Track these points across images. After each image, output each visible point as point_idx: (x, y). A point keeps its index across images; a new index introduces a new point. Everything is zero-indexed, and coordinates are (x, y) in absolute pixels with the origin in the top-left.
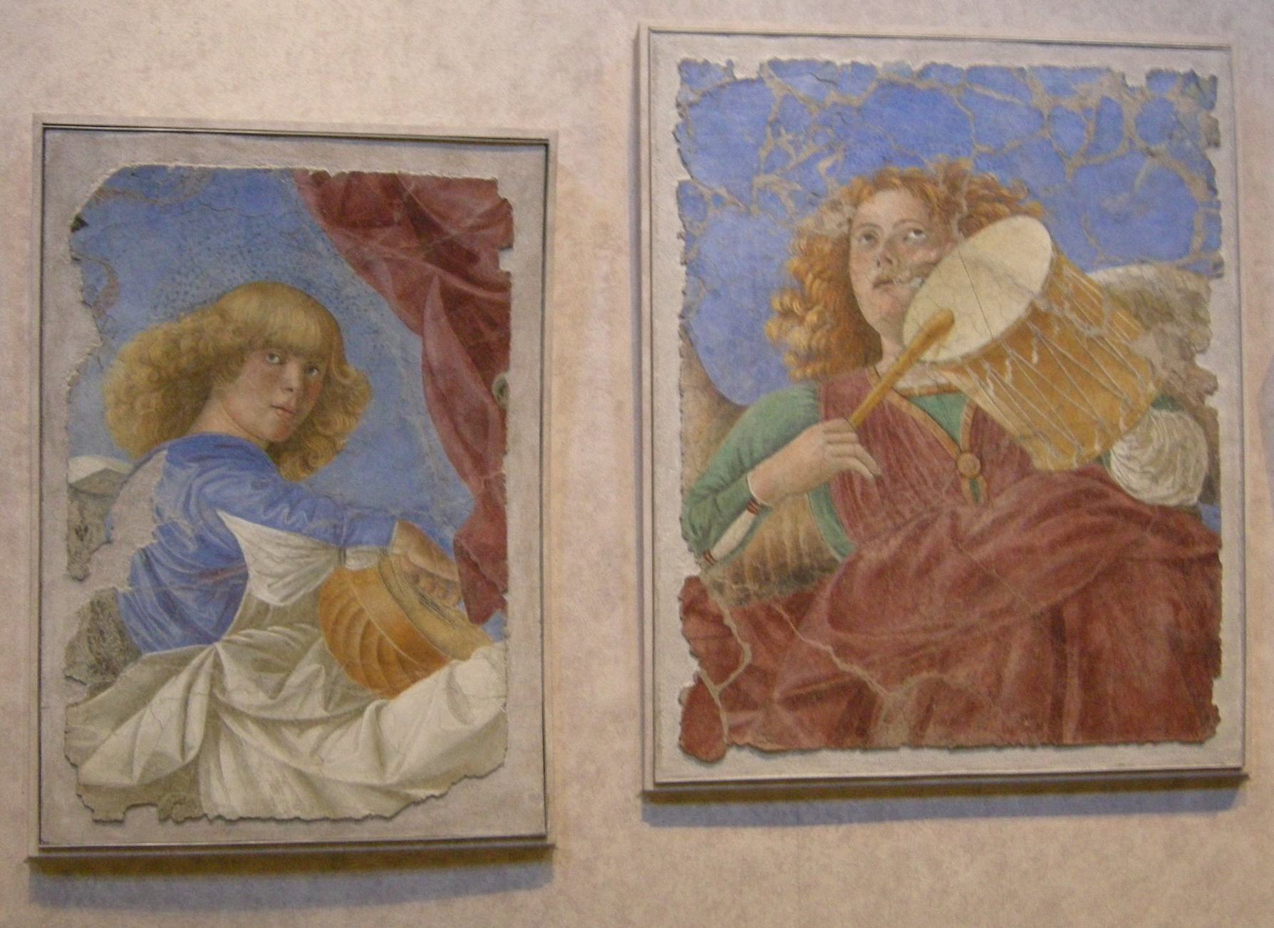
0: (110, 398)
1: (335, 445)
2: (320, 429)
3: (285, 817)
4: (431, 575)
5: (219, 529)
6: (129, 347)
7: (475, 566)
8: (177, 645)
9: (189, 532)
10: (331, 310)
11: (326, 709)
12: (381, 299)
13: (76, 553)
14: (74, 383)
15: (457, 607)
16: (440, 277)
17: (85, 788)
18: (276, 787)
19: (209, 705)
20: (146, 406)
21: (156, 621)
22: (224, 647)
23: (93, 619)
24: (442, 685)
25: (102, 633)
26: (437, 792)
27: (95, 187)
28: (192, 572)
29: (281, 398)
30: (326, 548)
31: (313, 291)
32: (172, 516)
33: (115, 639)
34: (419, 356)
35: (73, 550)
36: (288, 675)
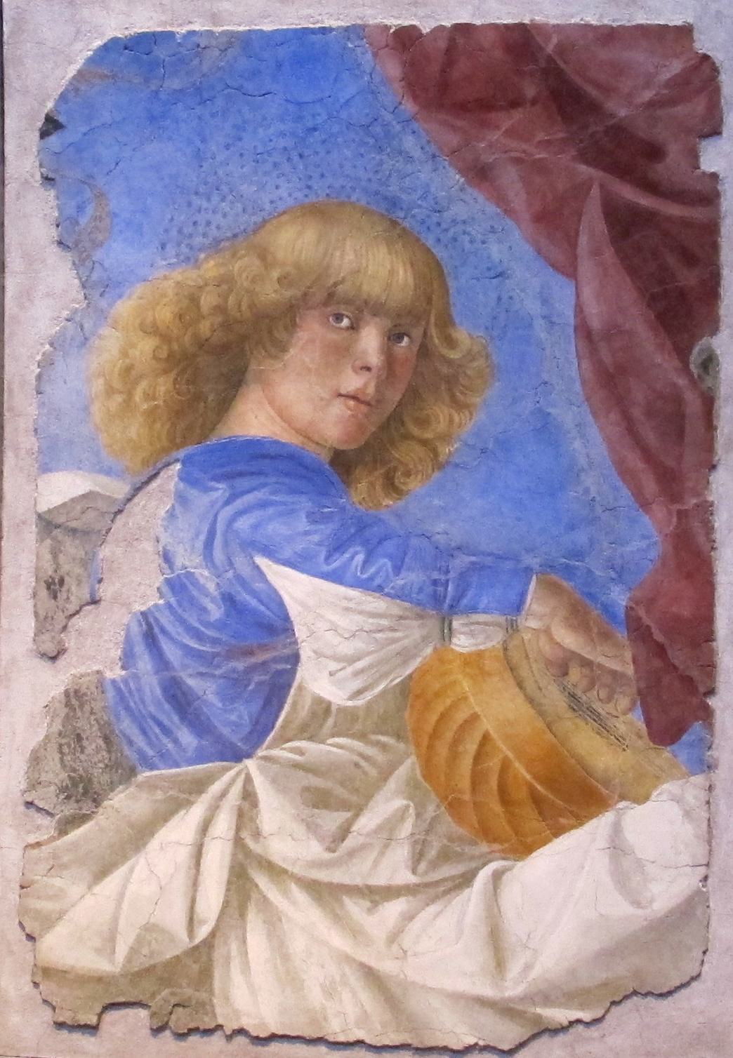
0: (98, 385)
1: (436, 453)
2: (415, 431)
3: (342, 1038)
4: (586, 663)
5: (258, 586)
6: (125, 307)
7: (661, 651)
8: (191, 762)
9: (211, 587)
10: (430, 242)
11: (414, 872)
12: (509, 223)
13: (46, 618)
14: (47, 363)
15: (630, 716)
16: (602, 186)
17: (45, 973)
18: (330, 991)
19: (234, 855)
20: (148, 397)
21: (160, 724)
22: (260, 768)
23: (67, 716)
24: (602, 842)
25: (79, 738)
26: (586, 1016)
27: (72, 71)
28: (217, 649)
29: (353, 382)
30: (420, 617)
31: (402, 214)
32: (187, 563)
33: (98, 750)
34: (570, 313)
35: (42, 613)
36: (357, 816)
